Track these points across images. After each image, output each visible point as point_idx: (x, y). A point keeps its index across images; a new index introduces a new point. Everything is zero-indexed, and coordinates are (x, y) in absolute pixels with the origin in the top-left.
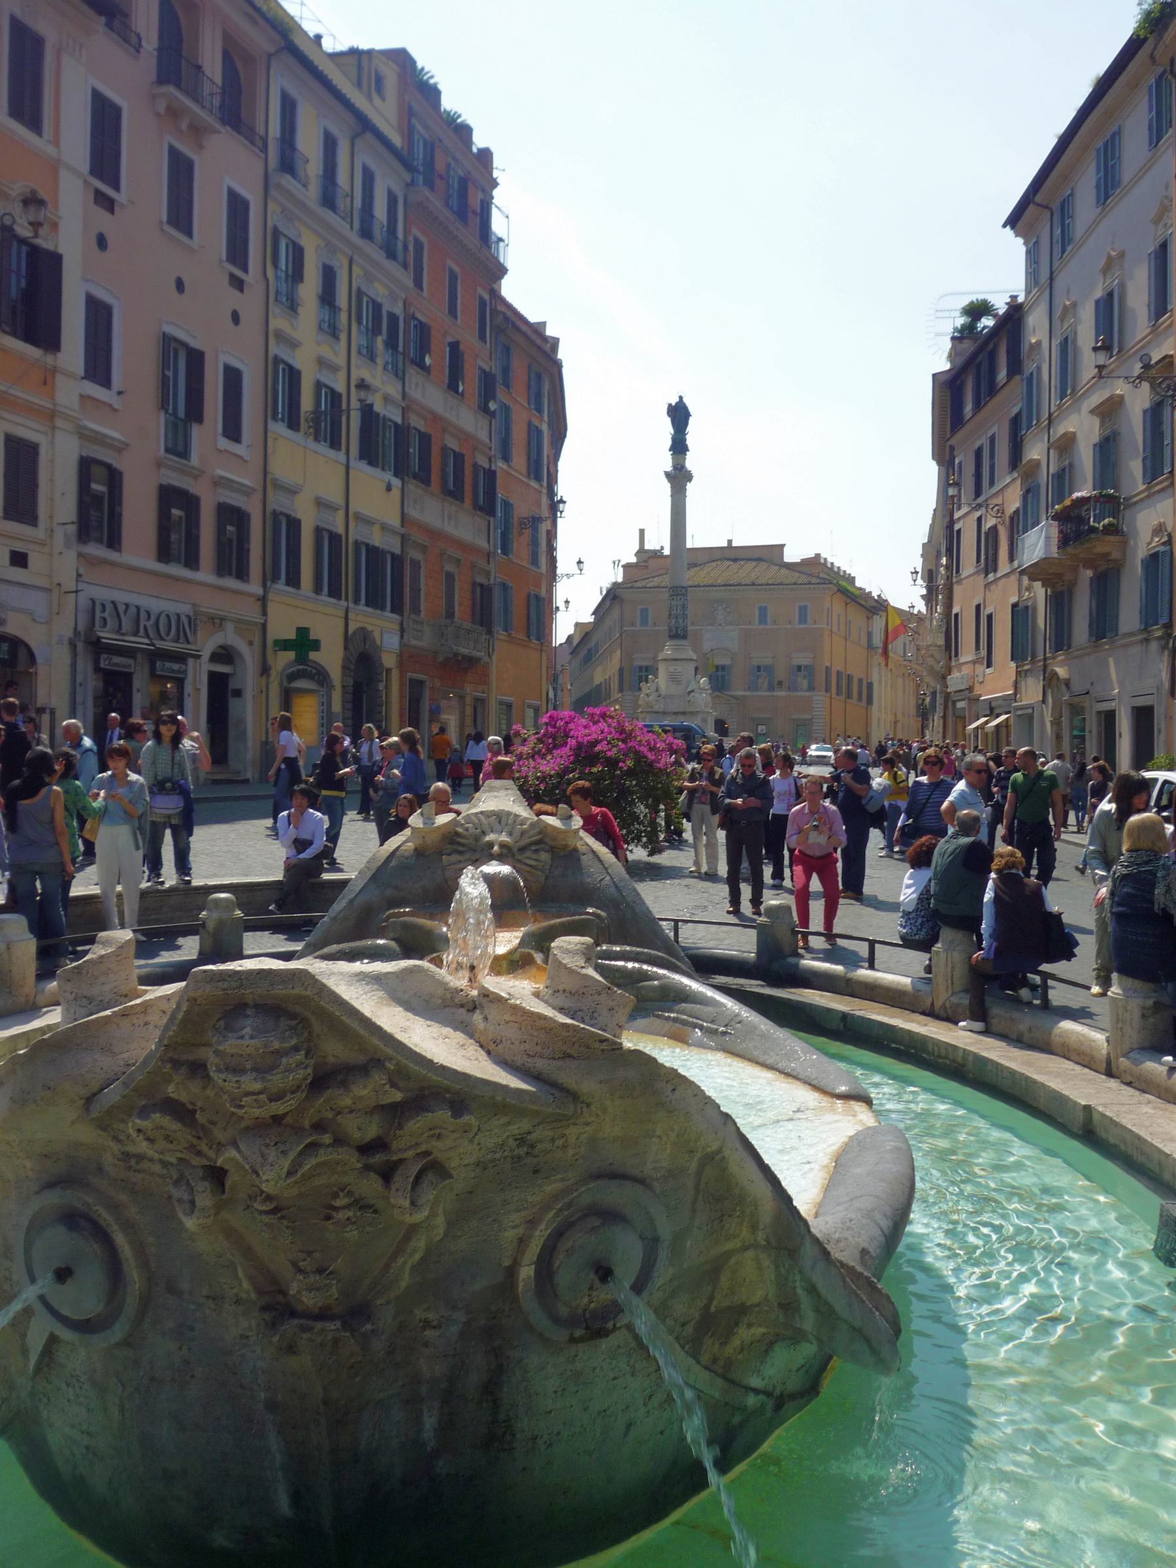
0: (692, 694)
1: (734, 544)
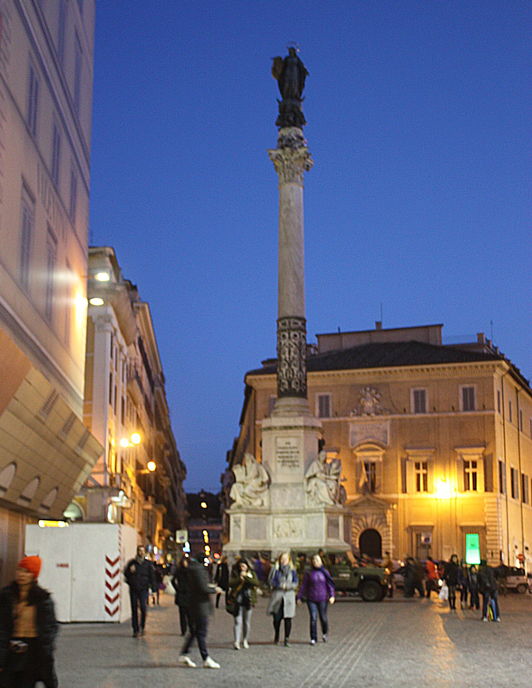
0: (313, 481)
1: (384, 327)
